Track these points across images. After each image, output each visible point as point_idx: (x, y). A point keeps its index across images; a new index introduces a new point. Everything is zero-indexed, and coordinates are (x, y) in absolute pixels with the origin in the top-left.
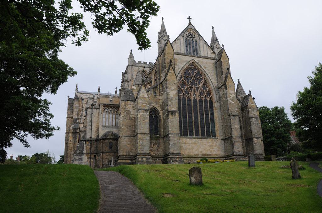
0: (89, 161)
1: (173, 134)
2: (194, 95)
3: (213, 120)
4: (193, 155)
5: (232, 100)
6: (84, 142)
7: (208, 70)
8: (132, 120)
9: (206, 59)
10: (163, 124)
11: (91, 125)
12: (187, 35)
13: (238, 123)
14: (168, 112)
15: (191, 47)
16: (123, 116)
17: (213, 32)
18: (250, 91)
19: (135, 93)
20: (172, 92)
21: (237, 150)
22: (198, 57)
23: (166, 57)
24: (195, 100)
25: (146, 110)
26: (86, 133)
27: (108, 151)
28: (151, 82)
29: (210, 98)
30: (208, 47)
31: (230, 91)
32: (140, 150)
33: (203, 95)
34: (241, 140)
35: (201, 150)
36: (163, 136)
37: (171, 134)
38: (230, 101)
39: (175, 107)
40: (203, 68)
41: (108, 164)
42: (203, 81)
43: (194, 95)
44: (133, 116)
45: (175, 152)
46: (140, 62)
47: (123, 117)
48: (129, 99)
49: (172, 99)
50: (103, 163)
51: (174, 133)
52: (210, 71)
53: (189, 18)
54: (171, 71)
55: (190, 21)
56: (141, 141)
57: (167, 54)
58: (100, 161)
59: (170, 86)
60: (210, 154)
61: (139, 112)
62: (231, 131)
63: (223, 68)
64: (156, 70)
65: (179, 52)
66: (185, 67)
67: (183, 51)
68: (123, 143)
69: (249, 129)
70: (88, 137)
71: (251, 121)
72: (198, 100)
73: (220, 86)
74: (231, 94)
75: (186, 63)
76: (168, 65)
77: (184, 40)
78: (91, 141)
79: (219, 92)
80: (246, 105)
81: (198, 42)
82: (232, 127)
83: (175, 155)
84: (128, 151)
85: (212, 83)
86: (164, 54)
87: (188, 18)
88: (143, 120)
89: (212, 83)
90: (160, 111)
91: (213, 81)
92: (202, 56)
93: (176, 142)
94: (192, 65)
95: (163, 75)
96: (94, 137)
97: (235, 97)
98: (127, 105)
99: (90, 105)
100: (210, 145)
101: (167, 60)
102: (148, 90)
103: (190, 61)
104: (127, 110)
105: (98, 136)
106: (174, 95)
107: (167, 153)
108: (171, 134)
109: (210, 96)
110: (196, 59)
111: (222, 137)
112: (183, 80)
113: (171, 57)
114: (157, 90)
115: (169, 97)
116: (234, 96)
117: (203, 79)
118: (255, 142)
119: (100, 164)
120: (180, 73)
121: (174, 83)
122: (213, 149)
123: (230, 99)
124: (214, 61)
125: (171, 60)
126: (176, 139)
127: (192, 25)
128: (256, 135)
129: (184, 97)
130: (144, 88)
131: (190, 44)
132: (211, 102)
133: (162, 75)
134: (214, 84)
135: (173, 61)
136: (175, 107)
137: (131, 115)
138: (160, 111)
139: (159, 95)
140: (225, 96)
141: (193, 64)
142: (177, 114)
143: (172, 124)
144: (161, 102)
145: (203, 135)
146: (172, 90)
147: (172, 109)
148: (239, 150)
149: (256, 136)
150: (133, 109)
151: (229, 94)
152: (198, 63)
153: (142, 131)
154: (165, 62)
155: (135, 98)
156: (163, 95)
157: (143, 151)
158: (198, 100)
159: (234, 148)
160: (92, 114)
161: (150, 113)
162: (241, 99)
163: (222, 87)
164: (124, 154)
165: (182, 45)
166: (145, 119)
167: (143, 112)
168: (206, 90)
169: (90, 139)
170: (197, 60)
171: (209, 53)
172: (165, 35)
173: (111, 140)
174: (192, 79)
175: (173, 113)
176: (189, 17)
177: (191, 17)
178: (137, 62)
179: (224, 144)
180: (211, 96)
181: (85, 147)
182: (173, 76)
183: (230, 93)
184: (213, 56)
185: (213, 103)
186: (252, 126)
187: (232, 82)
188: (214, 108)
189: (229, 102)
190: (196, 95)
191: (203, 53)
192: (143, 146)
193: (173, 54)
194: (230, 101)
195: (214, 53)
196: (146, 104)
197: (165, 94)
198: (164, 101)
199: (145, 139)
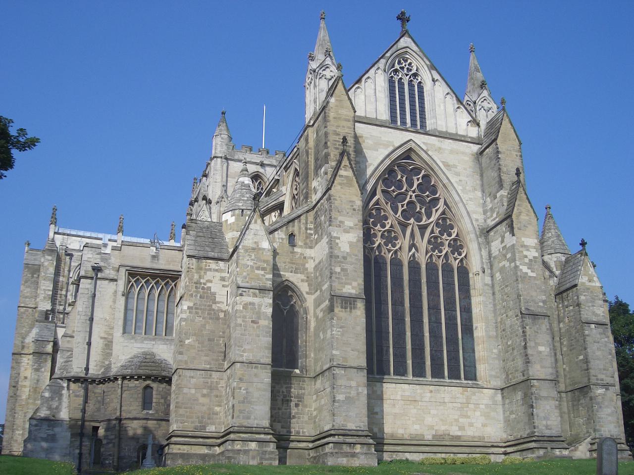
0: (78, 443)
1: (345, 367)
2: (413, 250)
3: (468, 329)
4: (406, 436)
5: (530, 265)
6: (65, 385)
7: (458, 174)
8: (218, 318)
10: (315, 334)
11: (88, 330)
13: (548, 338)
14: (332, 297)
16: (191, 304)
18: (583, 240)
19: (230, 236)
20: (347, 235)
21: (544, 422)
23: (331, 128)
24: (414, 266)
25: (262, 290)
26: (71, 356)
27: (138, 416)
28: (280, 207)
29: (462, 260)
31: (523, 239)
32: (238, 417)
33: (441, 251)
34: (554, 394)
35: (429, 420)
36: (312, 375)
37: (338, 366)
38: (525, 269)
39: (355, 284)
40: (442, 167)
41: (135, 454)
42: (441, 206)
43: (413, 249)
44: (224, 307)
45: (351, 426)
47: (189, 308)
48: (211, 254)
49: (345, 258)
50: (119, 452)
51: (348, 364)
52: (461, 178)
54: (346, 172)
56: (243, 386)
57: (334, 118)
58: (111, 445)
59: (340, 218)
60: (459, 433)
61: (241, 295)
62: (527, 362)
63: (504, 169)
64: (296, 169)
66: (388, 162)
67: (384, 115)
68: (185, 390)
69: (581, 357)
70: (77, 369)
71: (587, 332)
72: (423, 267)
73: (493, 222)
74: (527, 248)
75: (391, 149)
76: (337, 152)
78: (84, 381)
79: (488, 243)
80: (573, 283)
82: (530, 351)
83: (352, 436)
84: (202, 417)
85: (468, 213)
86: (325, 120)
87: (398, 18)
88: (253, 322)
89: (468, 213)
90: (307, 293)
91: (471, 207)
93: (353, 393)
94: (409, 158)
95: (317, 184)
96: (94, 371)
97: (540, 260)
98: (202, 273)
99: (90, 269)
100: (459, 405)
101: (332, 137)
102: (272, 228)
104: (203, 288)
105: (108, 368)
106: (351, 244)
107: (326, 429)
108: (338, 366)
109: (460, 254)
110: (419, 139)
111: (499, 383)
112: (377, 203)
113: (345, 129)
114: (300, 228)
115: (336, 252)
116: (536, 255)
117: (442, 202)
118: (599, 399)
119: (110, 455)
121: (354, 210)
122: (469, 420)
123: (525, 264)
124: (475, 148)
125: (345, 140)
126: (353, 384)
128: (600, 376)
129: (383, 254)
130: (259, 221)
132: (464, 272)
133: (314, 184)
134: (474, 216)
135: (351, 141)
136: (355, 284)
137: (215, 303)
138: (306, 296)
139: (306, 244)
140: (509, 256)
142: (361, 305)
143: (342, 335)
144: (310, 266)
145: (437, 372)
146: (346, 231)
147: (344, 290)
148: (549, 423)
149: (602, 380)
150: (223, 286)
151: (521, 249)
152: (426, 153)
153: (246, 357)
154: (326, 143)
155: (231, 250)
156: (316, 243)
157: (249, 418)
158: (423, 267)
159: (535, 417)
160: (94, 296)
161: (275, 299)
162: (556, 266)
163: (499, 227)
164: (189, 426)
166: (259, 318)
167: (255, 295)
168: (450, 235)
169: (83, 375)
170: (424, 143)
172: (330, 63)
173: (148, 382)
174: (408, 199)
175: (348, 302)
177: (407, 15)
179: (504, 405)
180: (463, 255)
181: (65, 399)
182: (351, 185)
183: (522, 246)
184: (473, 132)
185: (471, 275)
186: (589, 350)
187: (528, 211)
188: (472, 292)
189: (519, 274)
190: (417, 250)
191: (444, 124)
192: (250, 403)
193: (351, 119)
194: (525, 269)
195: (475, 122)
196: (263, 269)
197: (325, 240)
198: (320, 263)
199: (255, 380)
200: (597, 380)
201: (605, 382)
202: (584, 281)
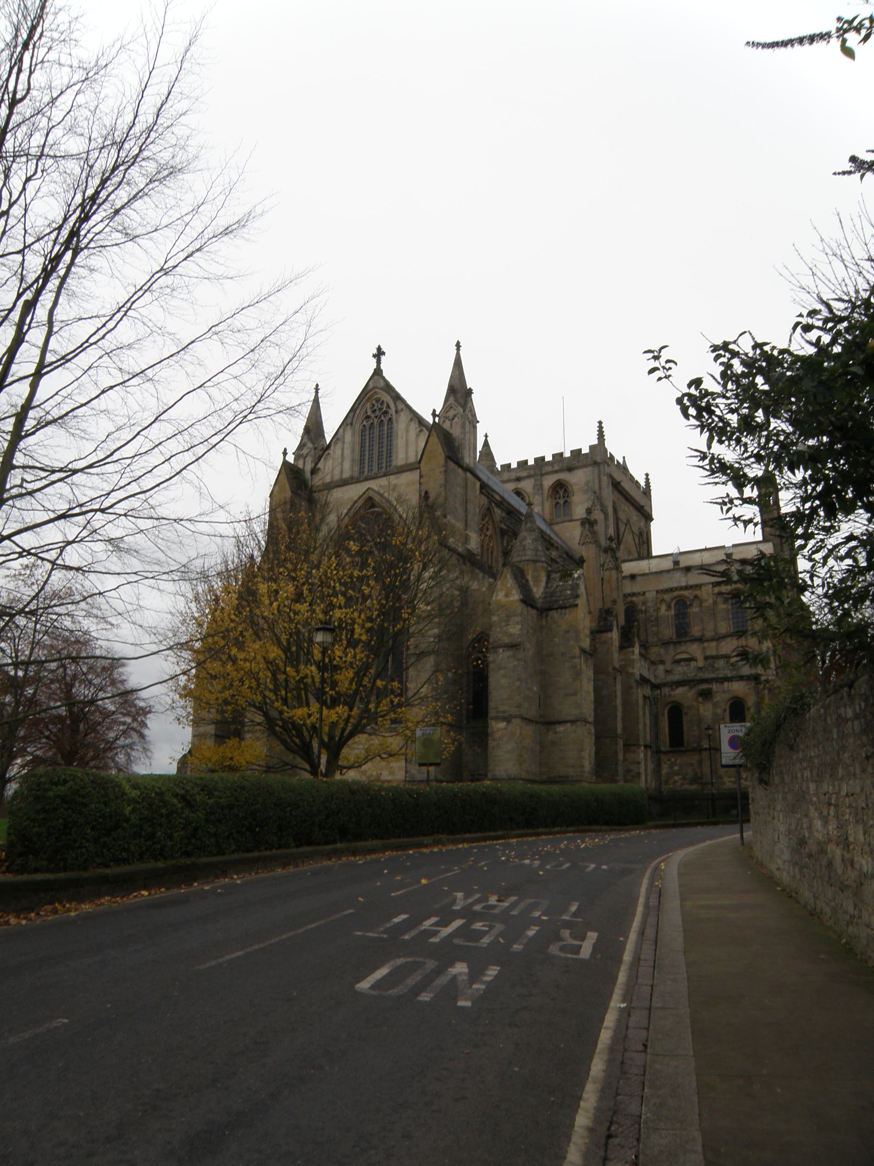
9: (408, 473)
15: (376, 447)
17: (458, 363)
30: (418, 430)
77: (353, 435)
110: (374, 484)
118: (498, 735)
131: (371, 440)
141: (369, 502)
149: (504, 712)
165: (347, 452)
200: (498, 712)
201: (507, 714)
202: (499, 598)
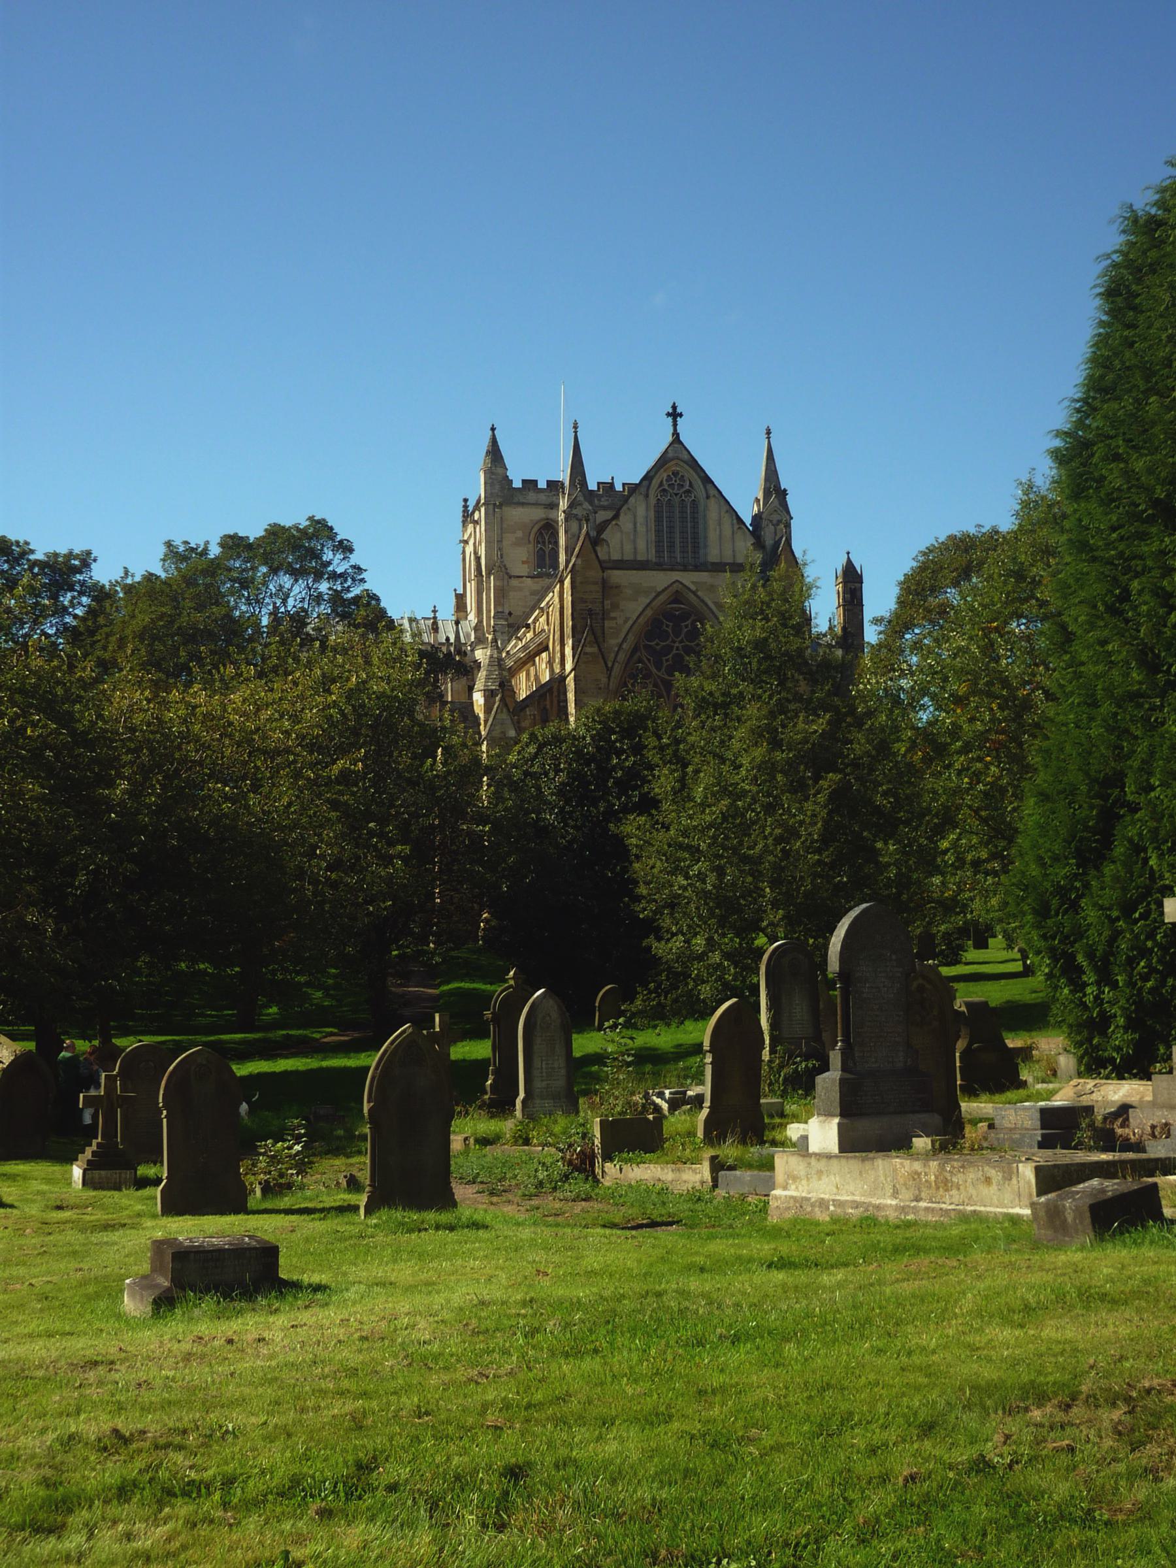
12: (661, 484)
22: (697, 568)
46: (530, 484)
53: (675, 414)
55: (675, 425)
65: (628, 556)
66: (649, 612)
67: (644, 548)
77: (647, 510)
81: (701, 508)
87: (668, 414)
92: (713, 564)
103: (666, 589)
110: (688, 579)
114: (552, 702)
120: (631, 638)
127: (681, 443)
141: (677, 598)
152: (694, 593)
165: (641, 529)
171: (744, 549)
174: (675, 652)
176: (674, 407)
177: (679, 410)
178: (517, 484)
